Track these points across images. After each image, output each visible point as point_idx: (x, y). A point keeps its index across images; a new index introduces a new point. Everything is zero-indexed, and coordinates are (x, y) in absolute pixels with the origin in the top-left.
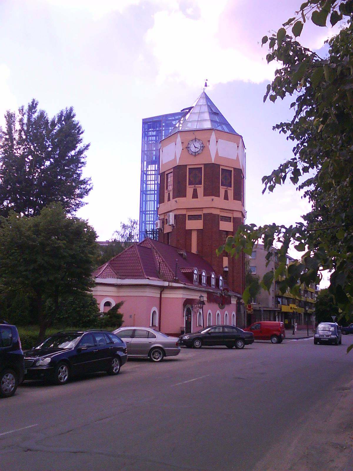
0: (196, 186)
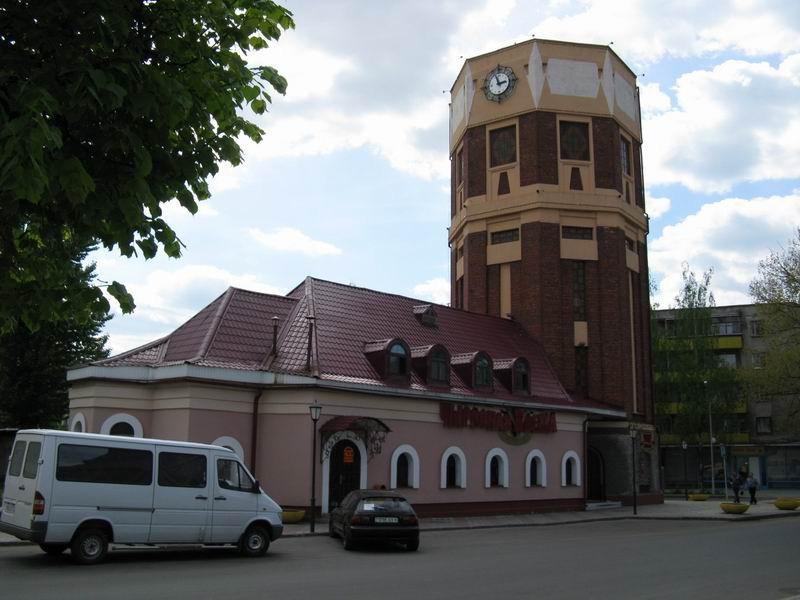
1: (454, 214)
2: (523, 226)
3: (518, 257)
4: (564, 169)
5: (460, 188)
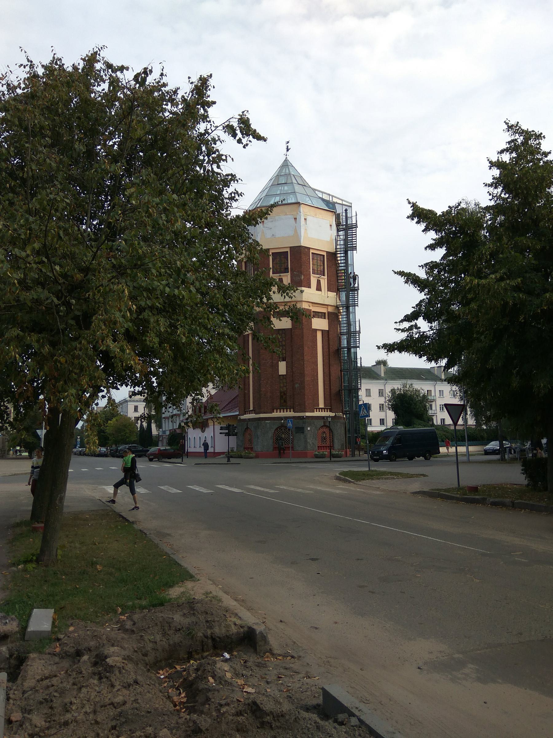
0: (281, 274)
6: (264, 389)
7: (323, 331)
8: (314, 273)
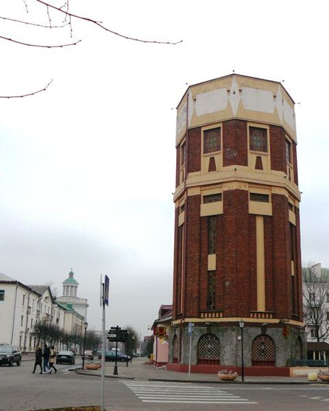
1: (178, 184)
2: (224, 192)
3: (221, 212)
4: (252, 158)
5: (183, 168)
6: (190, 289)
7: (265, 217)
8: (252, 148)
